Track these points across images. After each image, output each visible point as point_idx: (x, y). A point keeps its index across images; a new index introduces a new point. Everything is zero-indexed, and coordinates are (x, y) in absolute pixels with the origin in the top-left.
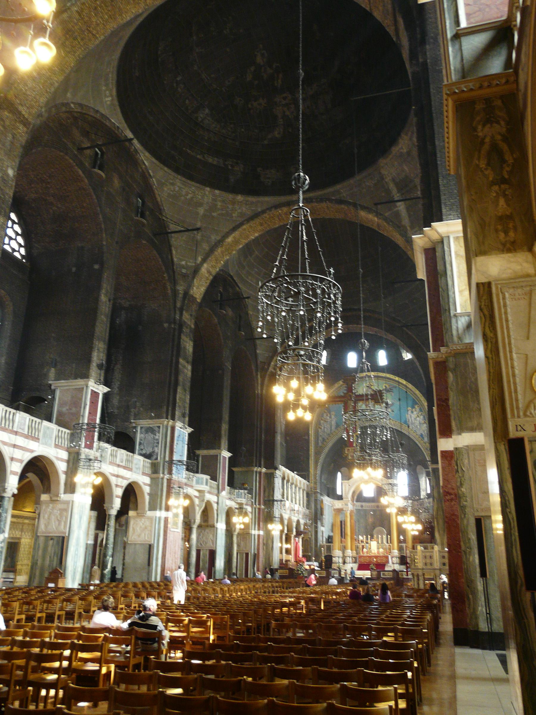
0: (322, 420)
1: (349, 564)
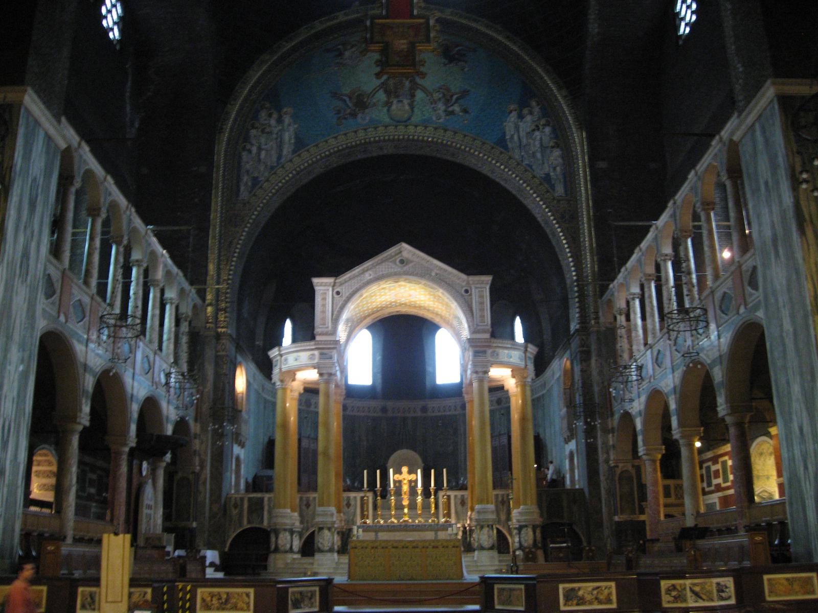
0: (253, 127)
1: (329, 554)
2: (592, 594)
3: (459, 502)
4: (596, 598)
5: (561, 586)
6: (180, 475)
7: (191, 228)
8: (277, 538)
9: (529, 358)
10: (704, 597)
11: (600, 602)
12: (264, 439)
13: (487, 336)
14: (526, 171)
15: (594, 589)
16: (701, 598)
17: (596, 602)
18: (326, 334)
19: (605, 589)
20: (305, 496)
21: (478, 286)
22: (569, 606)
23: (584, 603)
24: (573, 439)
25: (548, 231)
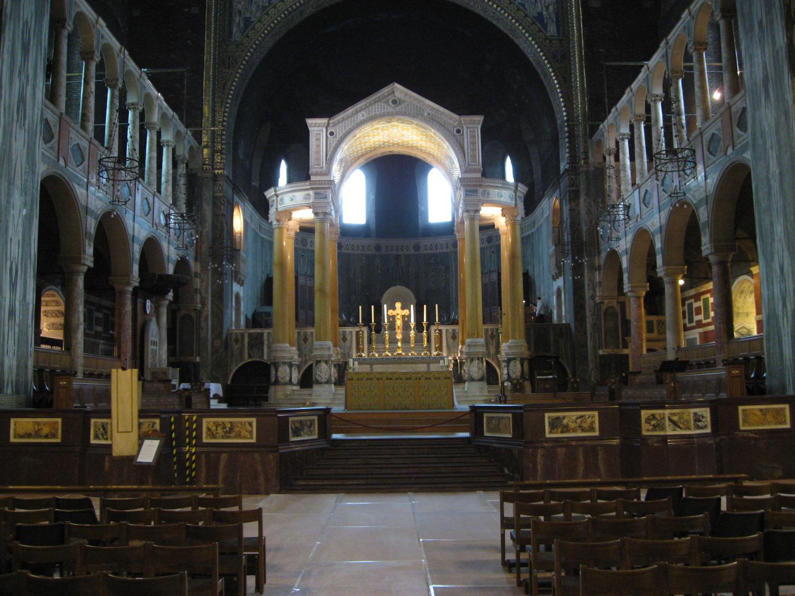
1: (327, 386)
2: (576, 422)
3: (450, 336)
4: (580, 427)
5: (547, 415)
6: (183, 312)
7: (185, 70)
8: (277, 371)
9: (519, 197)
10: (681, 426)
11: (583, 430)
12: (262, 277)
13: (479, 175)
14: (519, 9)
15: (578, 418)
16: (679, 427)
17: (579, 431)
18: (321, 174)
19: (589, 418)
20: (303, 331)
21: (469, 126)
22: (554, 433)
23: (568, 431)
24: (561, 276)
25: (539, 71)
